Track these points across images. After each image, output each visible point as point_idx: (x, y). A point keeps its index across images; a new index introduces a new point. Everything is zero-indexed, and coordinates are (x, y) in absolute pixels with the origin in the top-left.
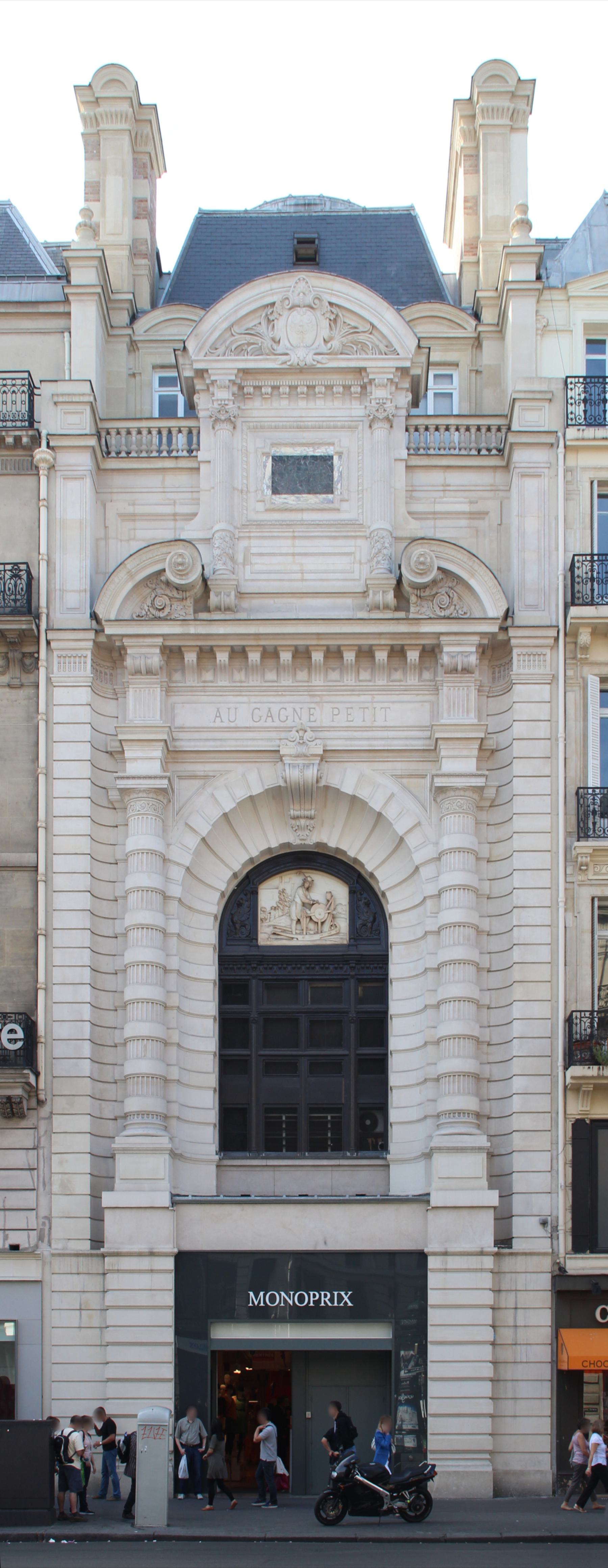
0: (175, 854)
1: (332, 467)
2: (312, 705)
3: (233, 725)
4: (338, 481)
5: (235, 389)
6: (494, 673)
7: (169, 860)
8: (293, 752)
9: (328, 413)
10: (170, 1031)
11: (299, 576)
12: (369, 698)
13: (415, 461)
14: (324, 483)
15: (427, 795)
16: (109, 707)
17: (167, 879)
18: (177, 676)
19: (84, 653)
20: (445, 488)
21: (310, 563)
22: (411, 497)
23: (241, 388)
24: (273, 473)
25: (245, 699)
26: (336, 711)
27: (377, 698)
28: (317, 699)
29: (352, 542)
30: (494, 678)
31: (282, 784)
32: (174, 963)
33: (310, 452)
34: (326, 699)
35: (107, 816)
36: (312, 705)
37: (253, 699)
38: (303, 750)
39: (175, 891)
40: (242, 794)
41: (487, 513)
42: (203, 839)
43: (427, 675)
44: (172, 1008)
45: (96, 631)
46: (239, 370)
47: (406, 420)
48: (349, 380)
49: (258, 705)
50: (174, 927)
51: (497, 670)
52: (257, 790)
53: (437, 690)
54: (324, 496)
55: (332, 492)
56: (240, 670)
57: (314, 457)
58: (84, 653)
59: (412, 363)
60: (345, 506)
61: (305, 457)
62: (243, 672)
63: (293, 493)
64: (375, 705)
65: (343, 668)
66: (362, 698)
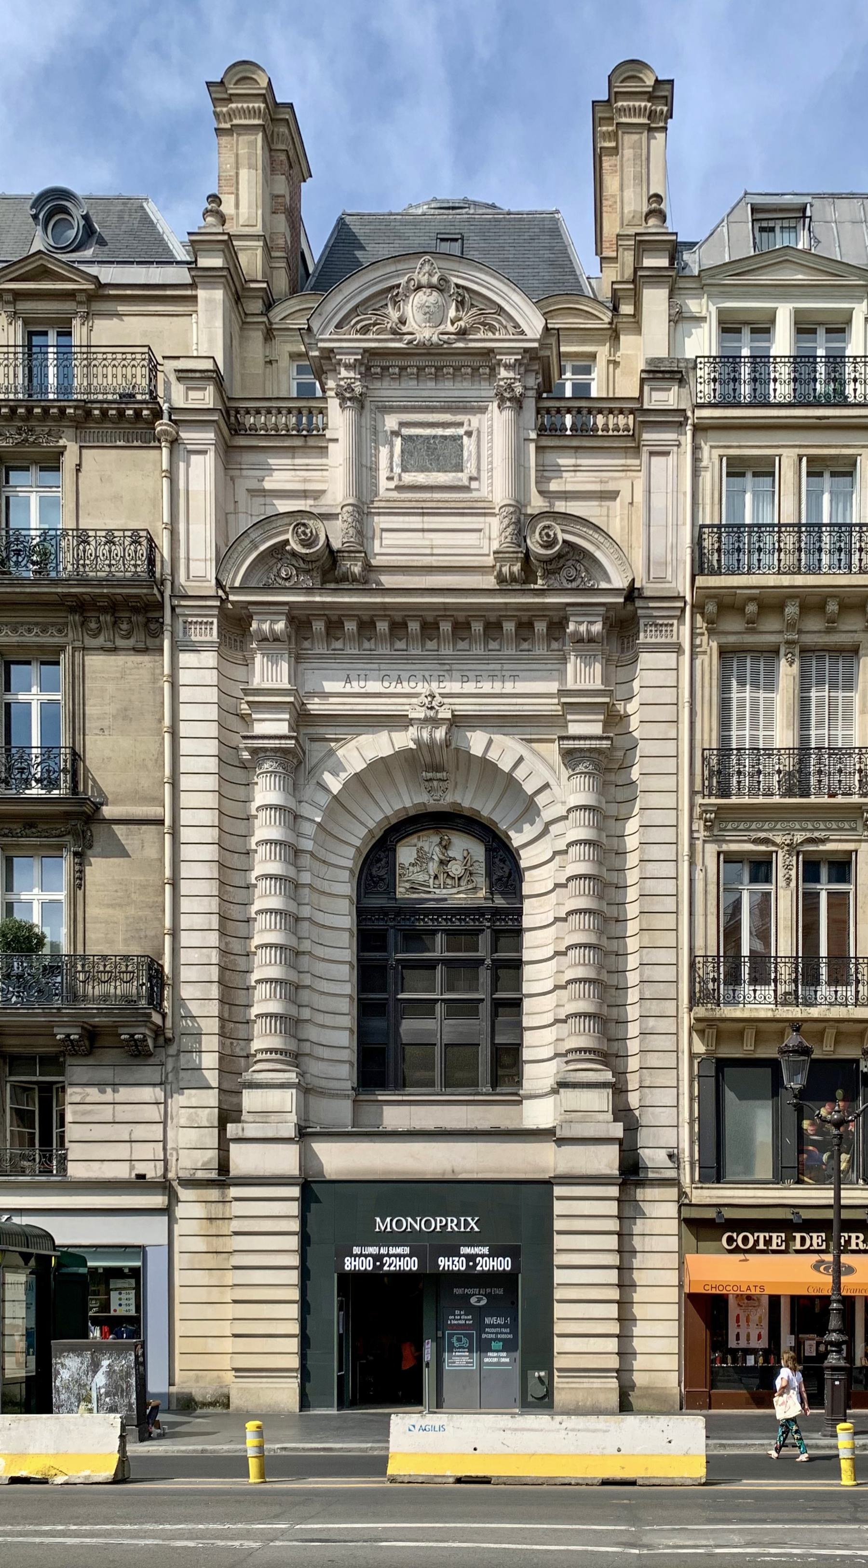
0: (306, 810)
1: (461, 446)
2: (442, 673)
3: (363, 691)
4: (468, 461)
5: (363, 369)
6: (623, 643)
7: (302, 817)
8: (422, 716)
9: (457, 393)
10: (302, 975)
11: (428, 551)
12: (499, 667)
13: (545, 442)
14: (454, 462)
15: (556, 758)
16: (239, 673)
17: (299, 835)
18: (306, 644)
19: (210, 620)
20: (576, 469)
21: (439, 539)
22: (542, 476)
23: (368, 368)
24: (402, 452)
25: (375, 666)
26: (465, 679)
27: (506, 667)
28: (447, 667)
29: (481, 519)
30: (623, 649)
31: (413, 746)
32: (306, 912)
33: (440, 432)
34: (455, 667)
35: (238, 775)
36: (442, 673)
37: (383, 666)
38: (432, 713)
39: (307, 845)
40: (371, 754)
41: (618, 492)
42: (335, 797)
43: (555, 645)
44: (304, 953)
45: (222, 601)
46: (366, 350)
47: (537, 402)
48: (477, 362)
49: (388, 673)
50: (306, 878)
51: (626, 641)
52: (387, 751)
53: (566, 659)
54: (454, 474)
55: (462, 471)
56: (369, 640)
57: (442, 436)
58: (210, 620)
59: (541, 345)
60: (474, 485)
61: (435, 437)
62: (373, 641)
63: (422, 471)
64: (504, 673)
65: (470, 638)
66: (491, 667)
